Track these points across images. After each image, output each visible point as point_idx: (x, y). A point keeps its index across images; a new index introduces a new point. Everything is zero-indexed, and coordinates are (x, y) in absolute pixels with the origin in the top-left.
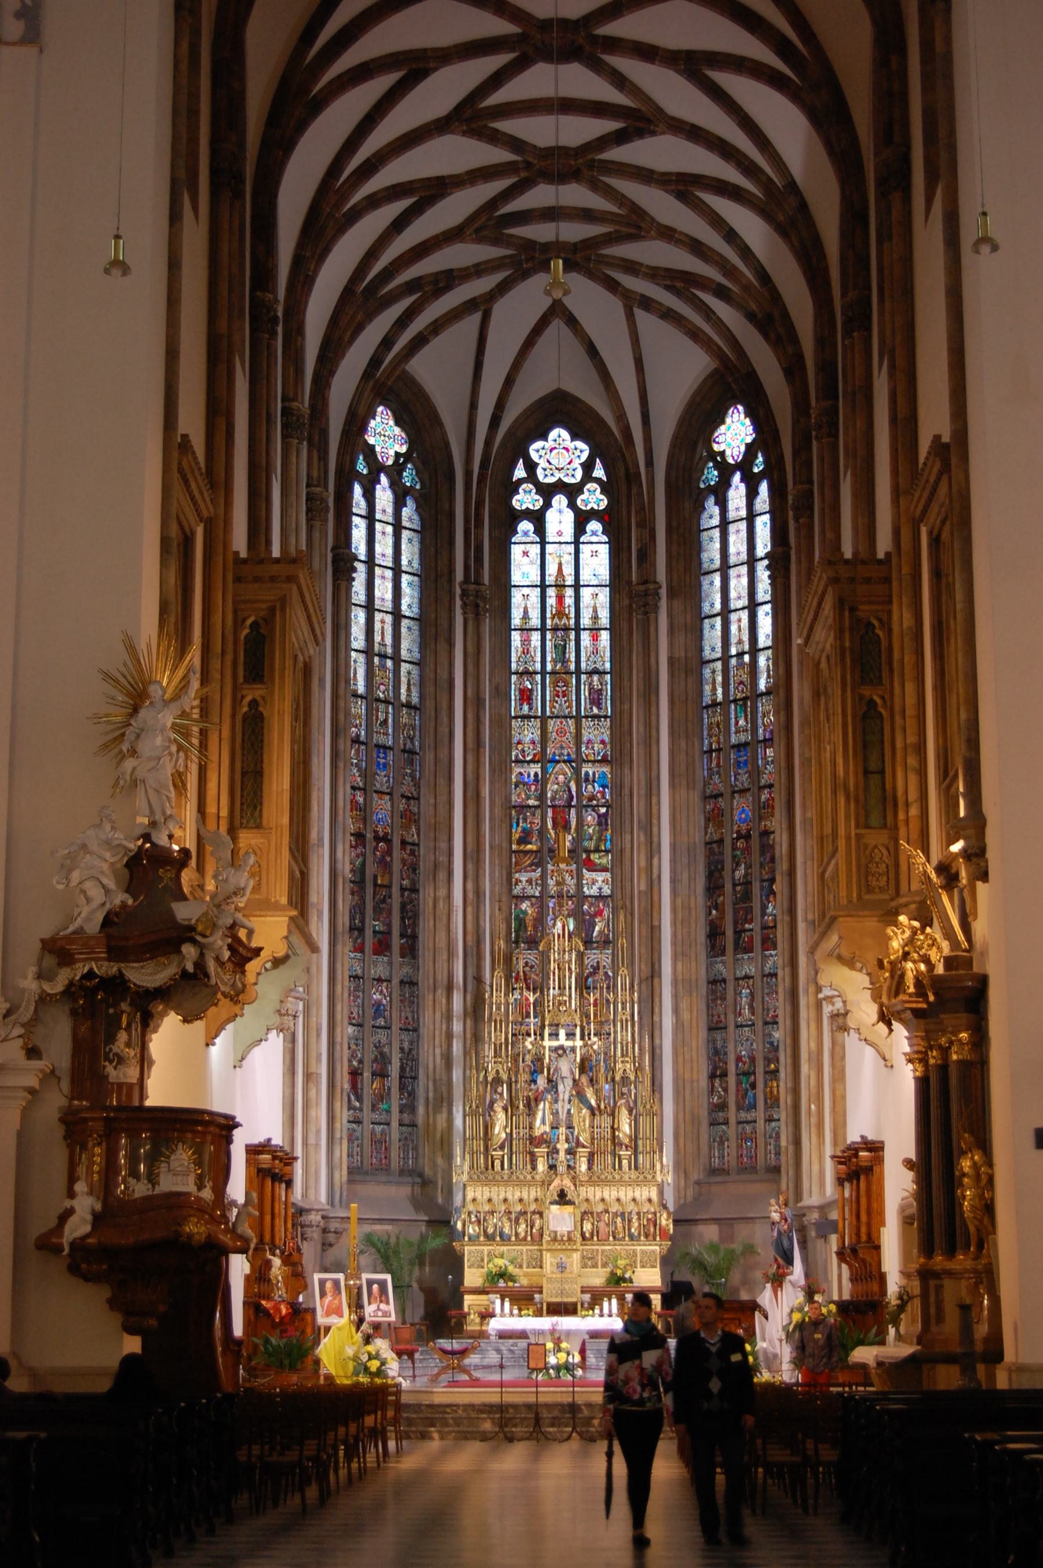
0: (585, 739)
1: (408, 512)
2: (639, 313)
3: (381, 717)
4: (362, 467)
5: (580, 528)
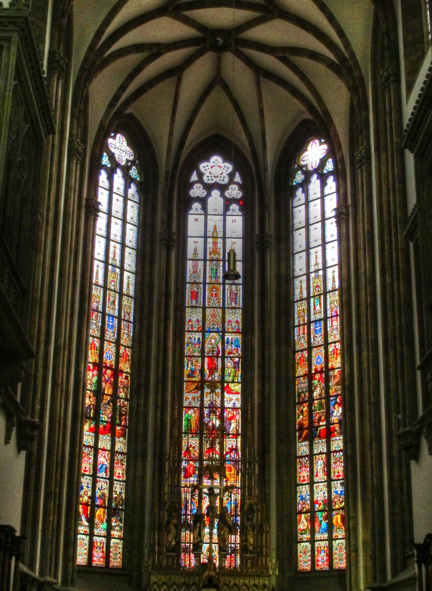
0: (227, 320)
1: (132, 190)
3: (112, 299)
4: (105, 160)
5: (226, 208)
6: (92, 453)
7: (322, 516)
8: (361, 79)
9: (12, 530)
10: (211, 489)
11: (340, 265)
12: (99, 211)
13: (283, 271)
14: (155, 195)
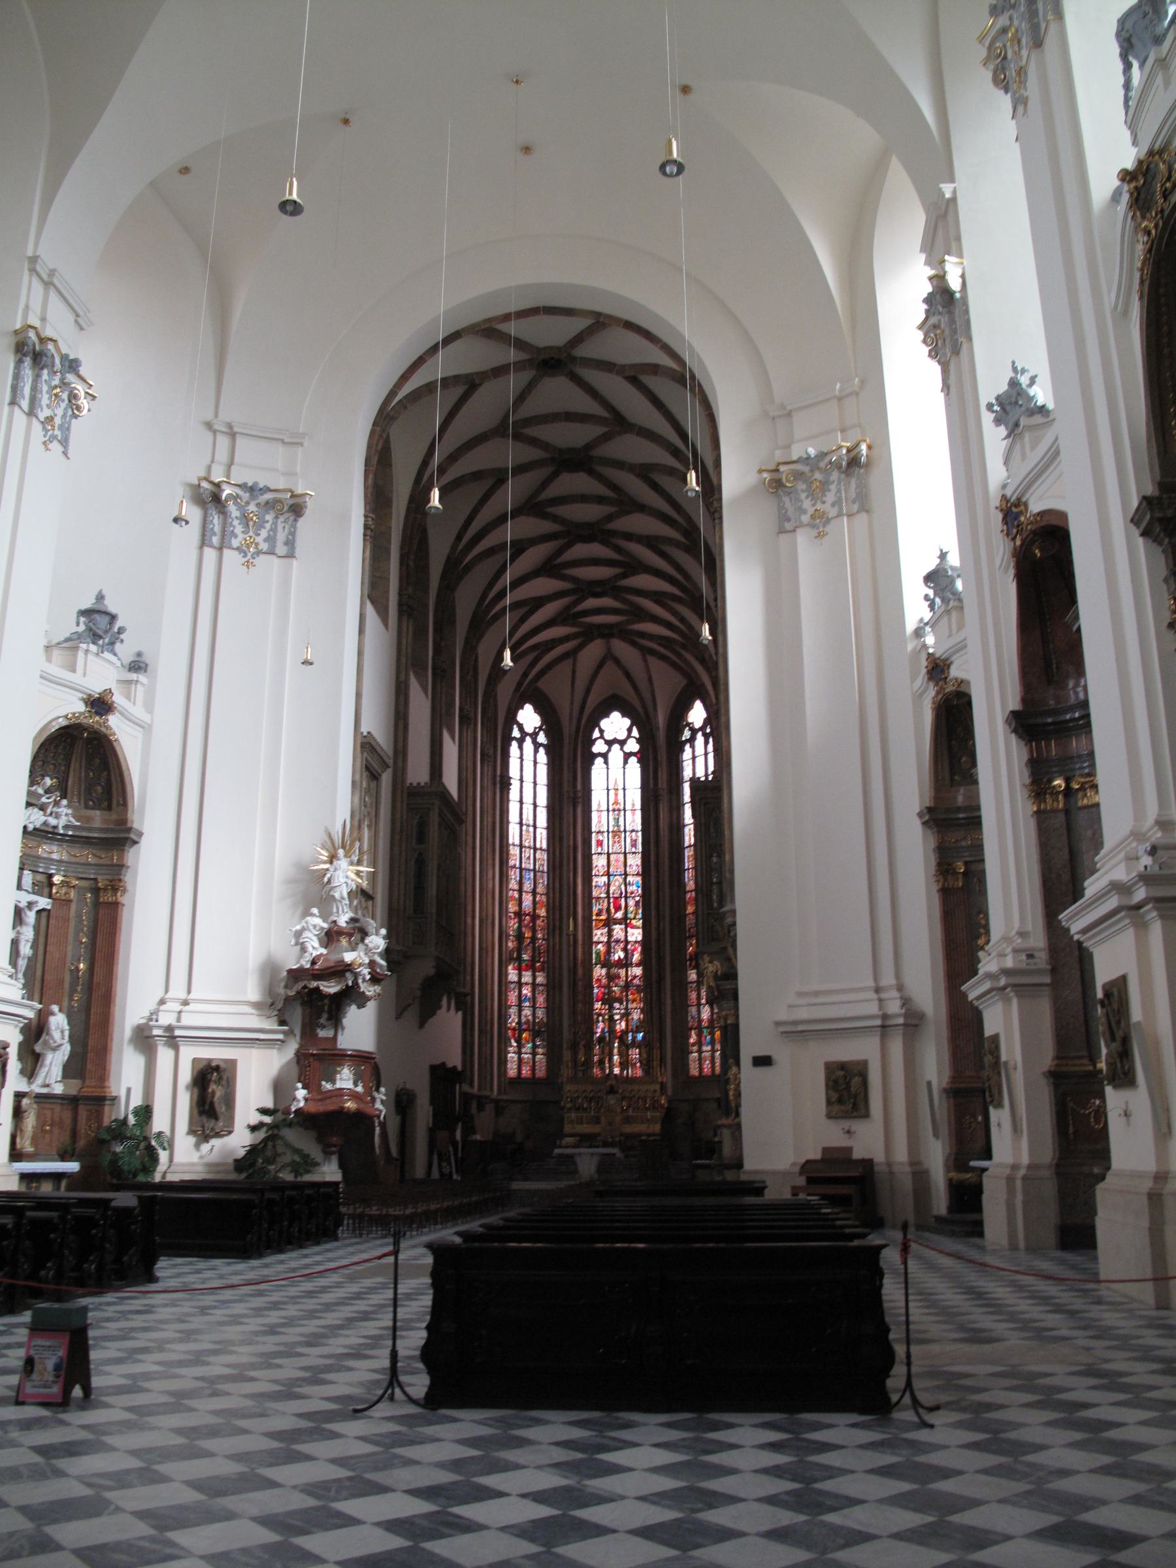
4: (516, 733)
5: (626, 762)
13: (675, 821)
14: (561, 756)
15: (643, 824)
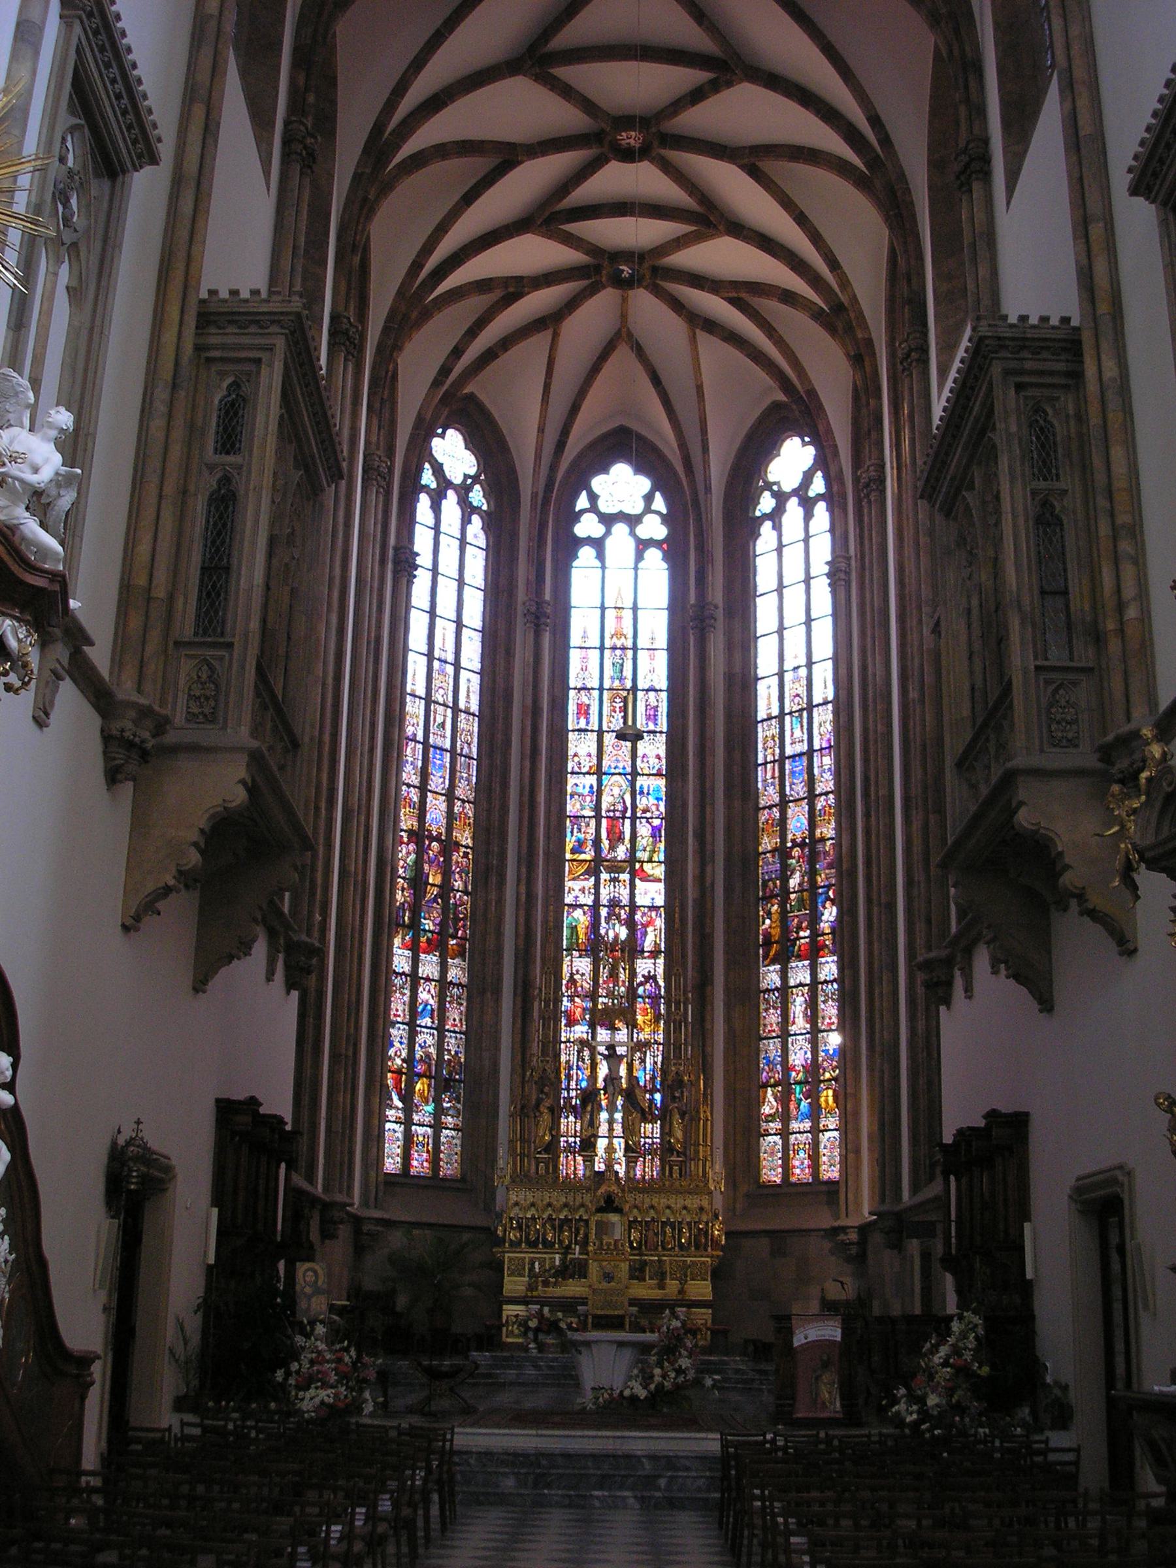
0: (640, 753)
2: (701, 336)
3: (439, 719)
4: (428, 478)
5: (639, 557)
6: (408, 985)
7: (801, 1091)
8: (869, 342)
9: (280, 1121)
10: (611, 1047)
11: (836, 659)
12: (416, 567)
13: (737, 669)
14: (514, 535)
15: (671, 677)
